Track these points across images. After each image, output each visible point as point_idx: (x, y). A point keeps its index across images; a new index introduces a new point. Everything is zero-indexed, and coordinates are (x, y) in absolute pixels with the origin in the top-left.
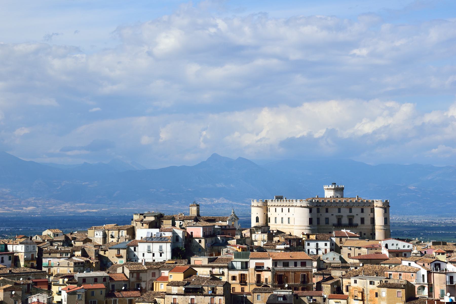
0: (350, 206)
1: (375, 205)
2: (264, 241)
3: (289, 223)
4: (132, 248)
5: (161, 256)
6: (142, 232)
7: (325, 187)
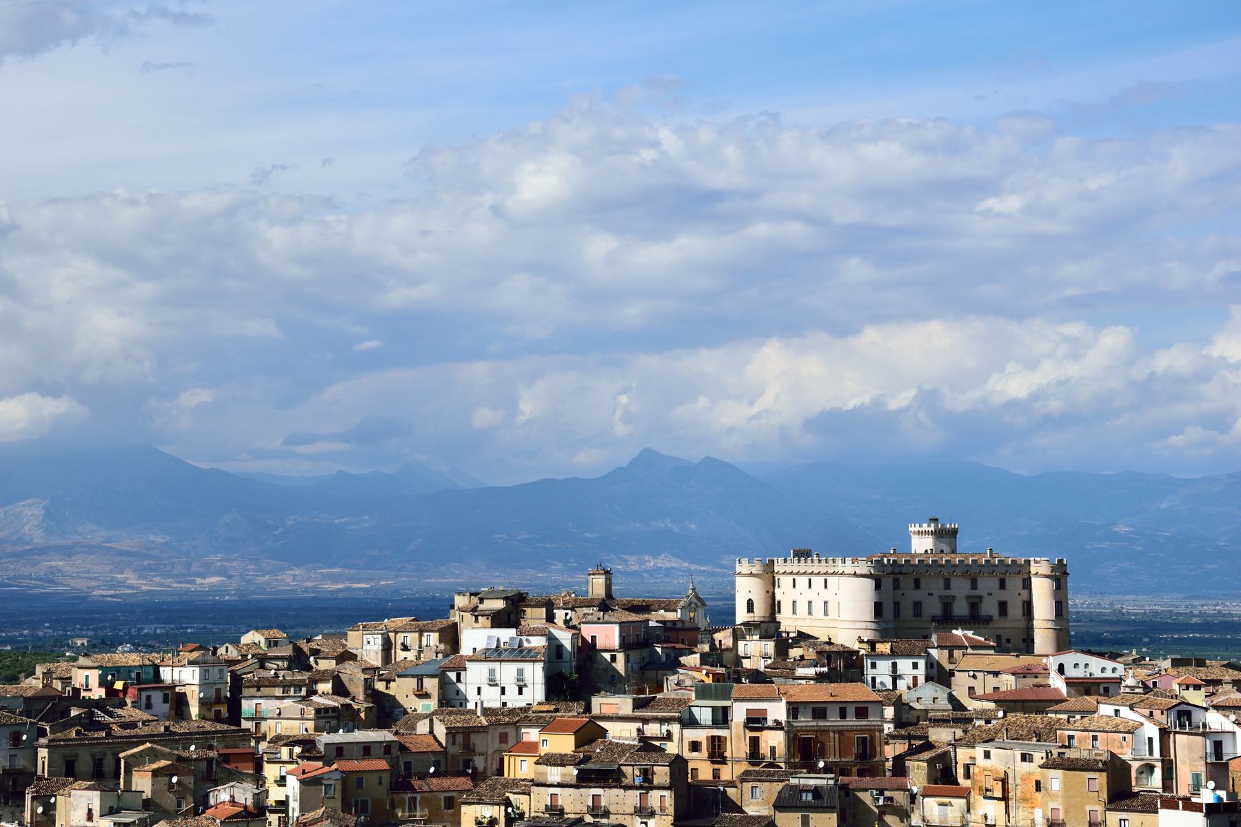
0: (972, 573)
1: (1033, 570)
2: (765, 657)
3: (826, 613)
4: (452, 676)
5: (520, 692)
6: (475, 637)
7: (913, 528)
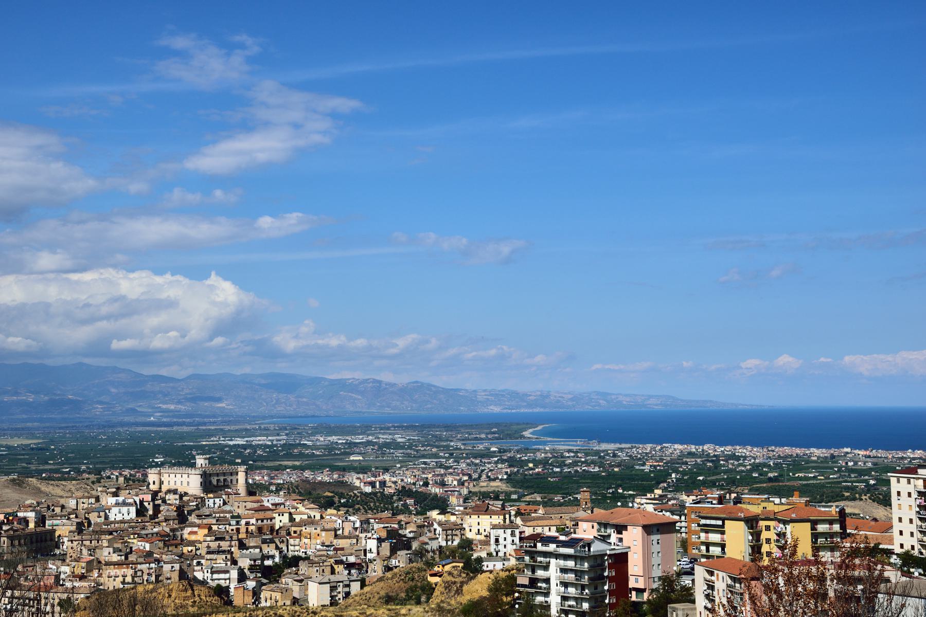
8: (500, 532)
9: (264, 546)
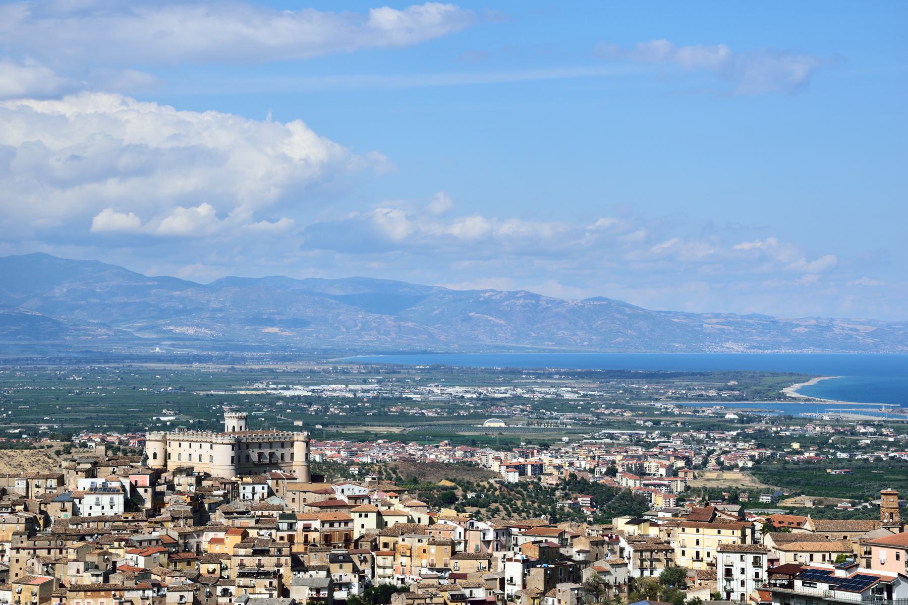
1: (295, 438)
2: (190, 485)
4: (77, 501)
8: (735, 558)
9: (334, 567)
